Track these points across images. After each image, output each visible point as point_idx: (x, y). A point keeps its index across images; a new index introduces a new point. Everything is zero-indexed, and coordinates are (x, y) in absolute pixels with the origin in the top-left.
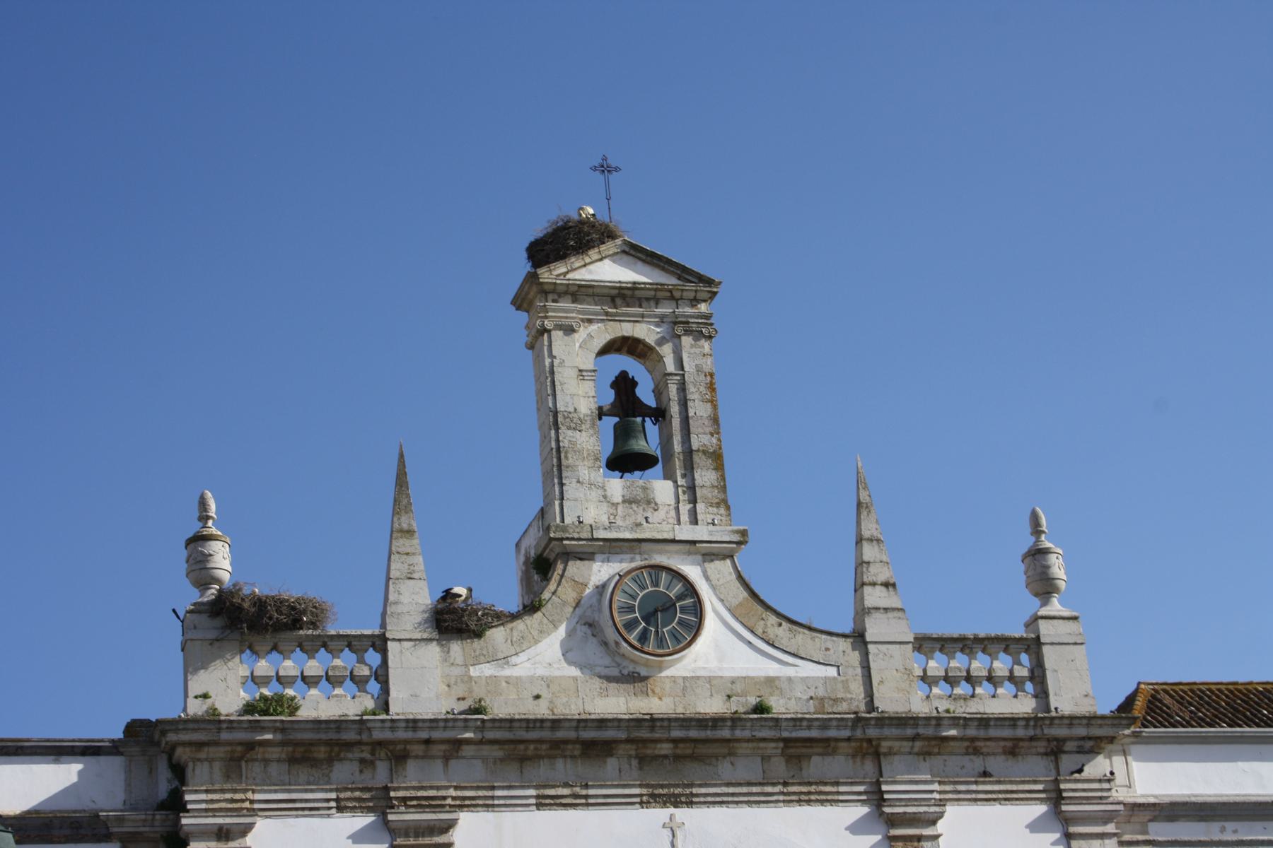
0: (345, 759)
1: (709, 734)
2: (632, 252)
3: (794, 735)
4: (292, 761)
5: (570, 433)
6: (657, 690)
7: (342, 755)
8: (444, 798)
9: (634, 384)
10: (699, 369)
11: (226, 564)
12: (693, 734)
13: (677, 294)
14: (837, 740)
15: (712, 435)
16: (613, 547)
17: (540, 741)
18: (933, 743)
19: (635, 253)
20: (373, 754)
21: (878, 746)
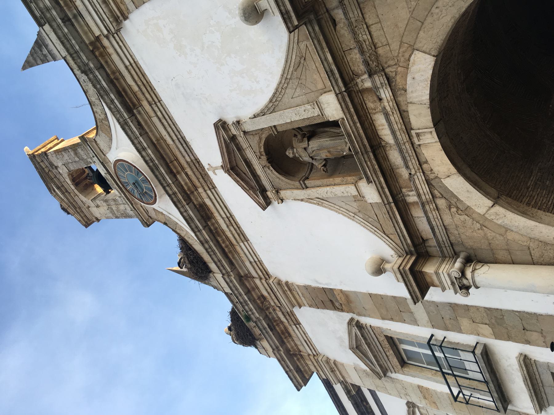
7: (277, 319)
20: (268, 309)
21: (92, 43)
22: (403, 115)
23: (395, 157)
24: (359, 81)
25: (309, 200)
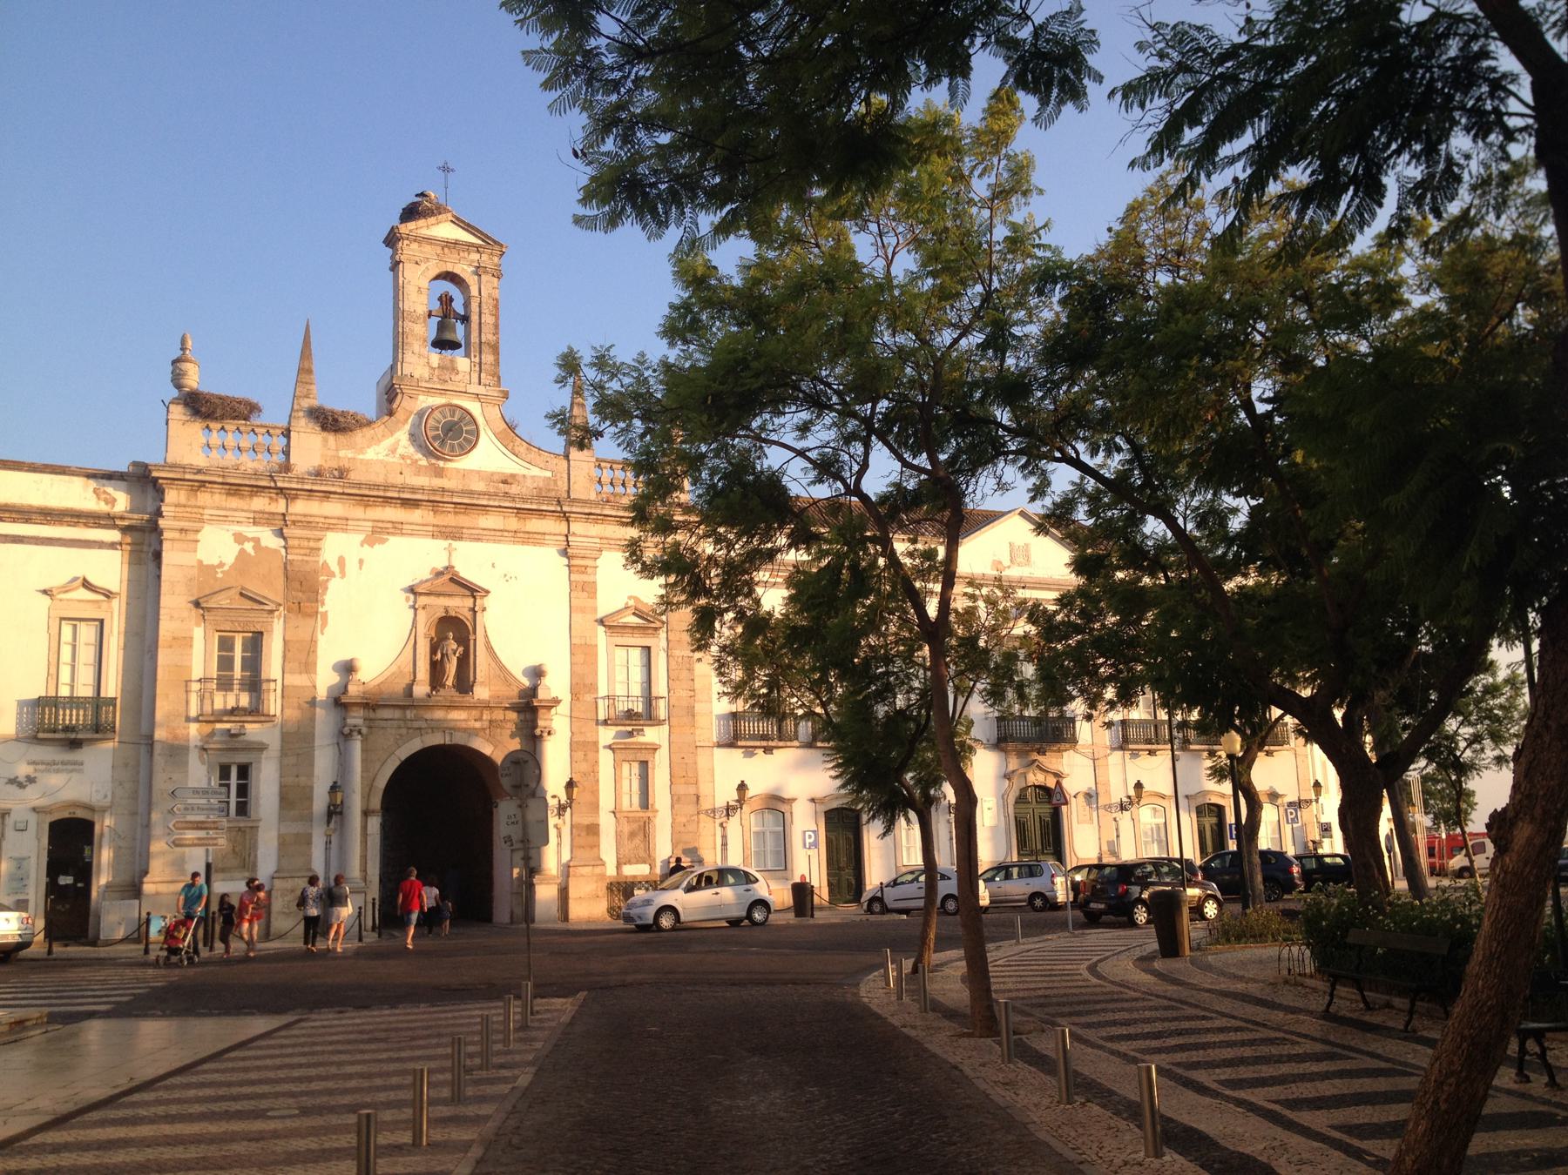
4: (228, 494)
9: (451, 300)
10: (490, 296)
11: (196, 378)
16: (430, 391)
19: (458, 222)
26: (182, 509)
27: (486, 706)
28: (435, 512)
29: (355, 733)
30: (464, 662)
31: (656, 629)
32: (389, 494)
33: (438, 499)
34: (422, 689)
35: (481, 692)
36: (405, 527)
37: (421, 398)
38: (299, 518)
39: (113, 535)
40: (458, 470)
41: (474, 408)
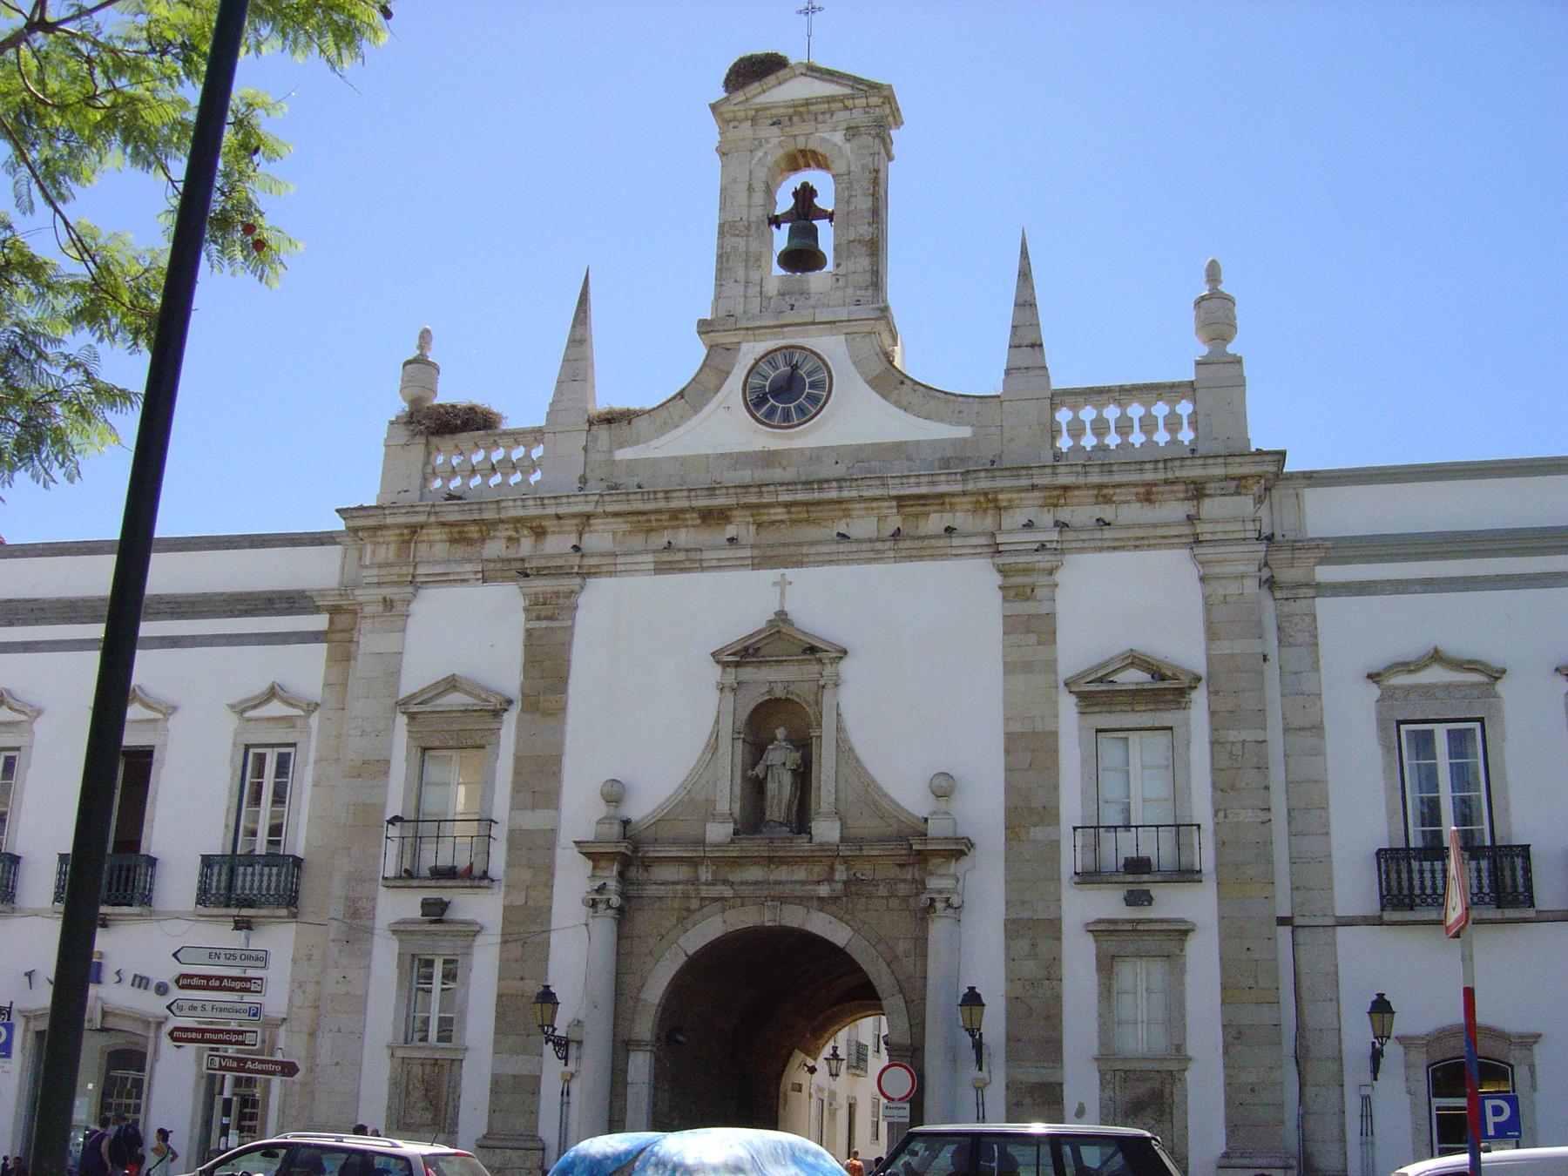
0: (494, 537)
1: (816, 496)
2: (809, 73)
3: (902, 492)
4: (452, 541)
5: (734, 239)
6: (784, 463)
8: (572, 567)
10: (864, 167)
12: (800, 497)
13: (849, 103)
14: (952, 495)
15: (869, 225)
16: (754, 331)
17: (657, 512)
18: (1055, 493)
20: (517, 532)
21: (996, 500)
22: (801, 901)
23: (755, 873)
24: (843, 868)
25: (716, 734)
26: (384, 572)
27: (829, 857)
28: (759, 525)
29: (602, 906)
30: (803, 776)
31: (1182, 692)
32: (674, 504)
33: (754, 500)
34: (719, 832)
35: (826, 830)
36: (707, 555)
37: (745, 347)
38: (543, 563)
39: (319, 622)
40: (801, 451)
41: (831, 347)
